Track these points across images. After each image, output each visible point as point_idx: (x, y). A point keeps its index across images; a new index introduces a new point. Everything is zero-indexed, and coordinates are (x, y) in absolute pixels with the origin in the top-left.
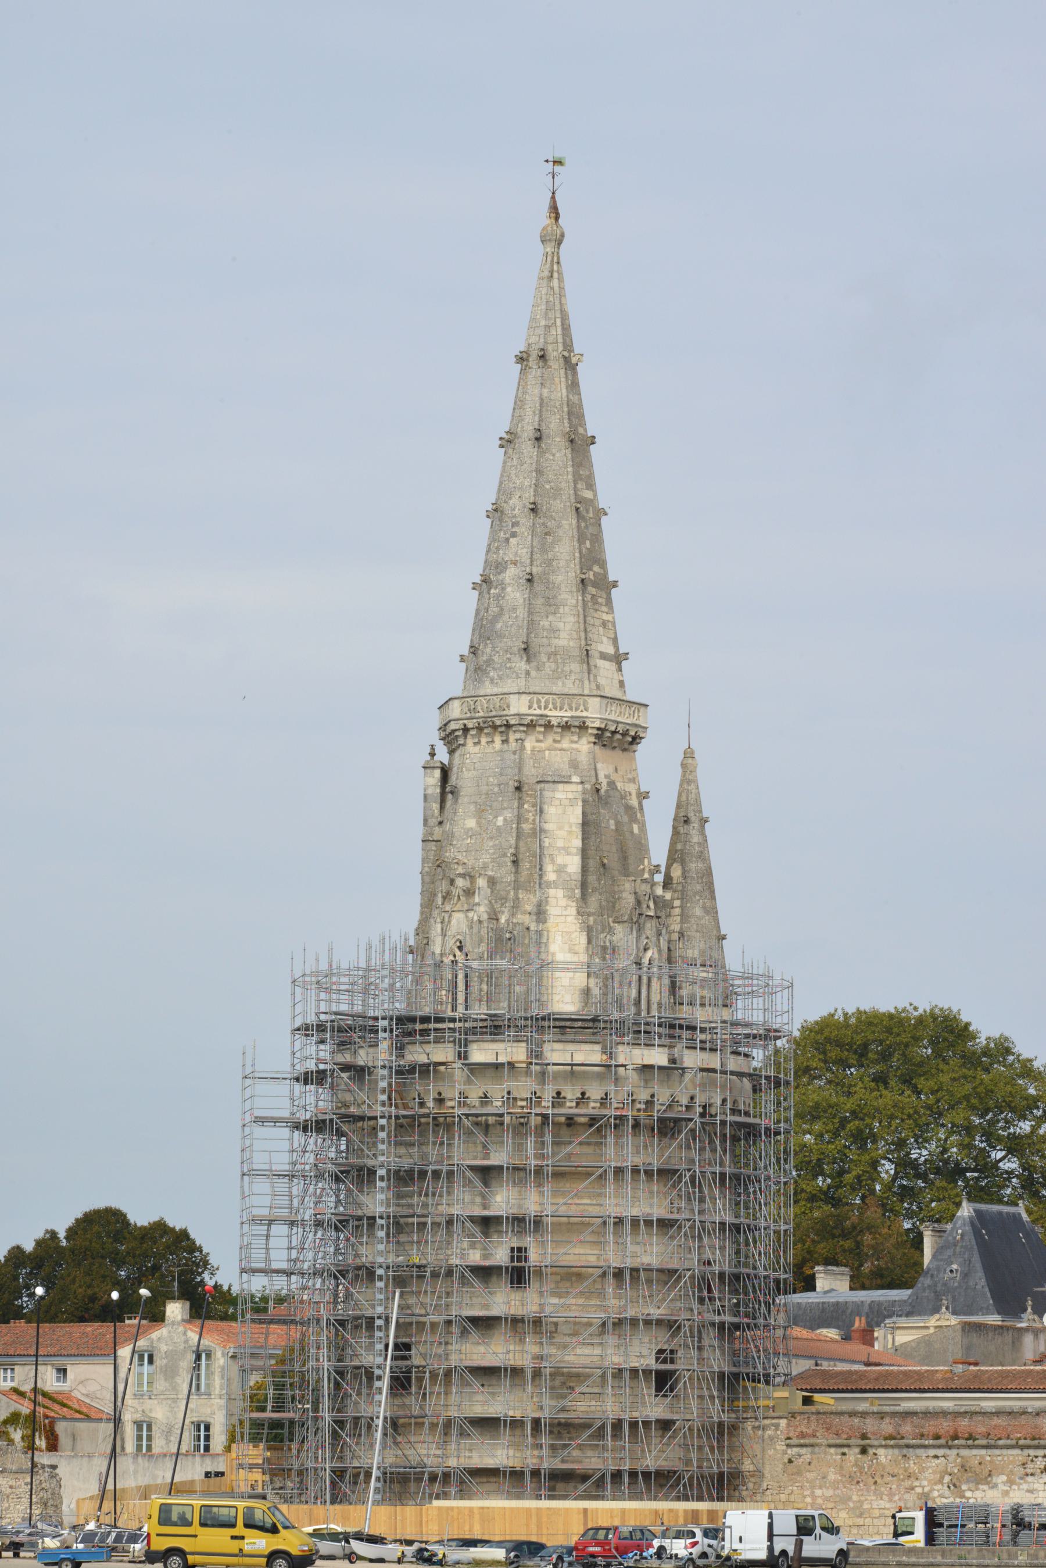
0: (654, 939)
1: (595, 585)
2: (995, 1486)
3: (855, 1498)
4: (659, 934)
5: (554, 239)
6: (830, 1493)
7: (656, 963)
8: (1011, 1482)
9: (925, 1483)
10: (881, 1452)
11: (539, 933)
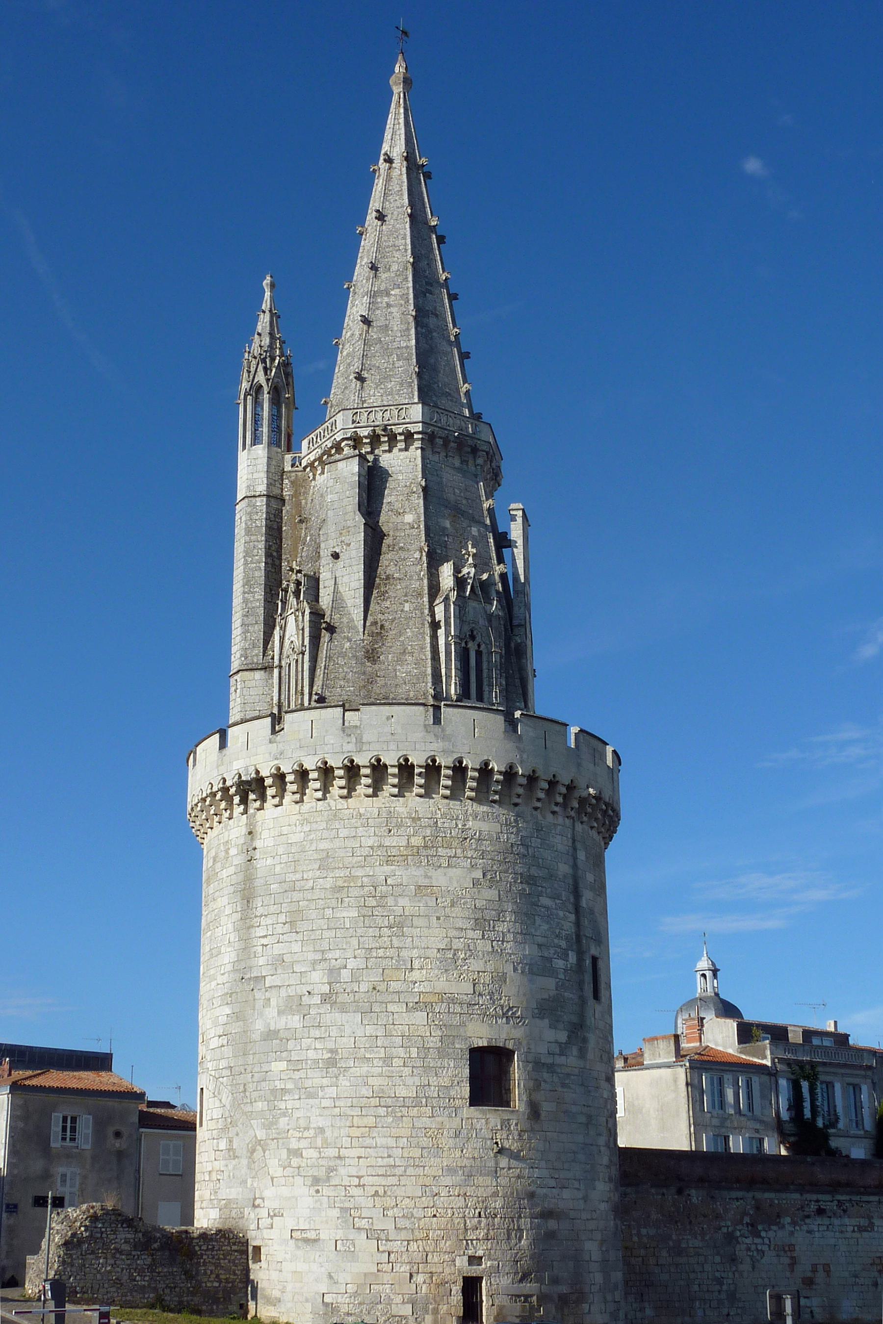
2: (783, 1227)
3: (674, 1237)
6: (652, 1232)
8: (794, 1223)
9: (729, 1223)
10: (693, 1192)
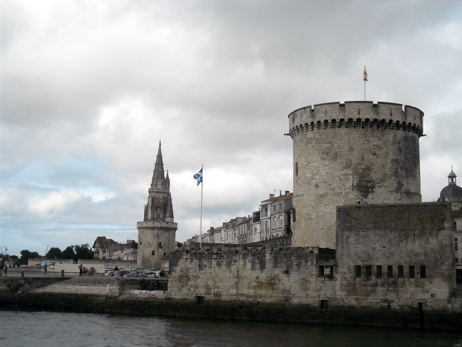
5: (160, 145)
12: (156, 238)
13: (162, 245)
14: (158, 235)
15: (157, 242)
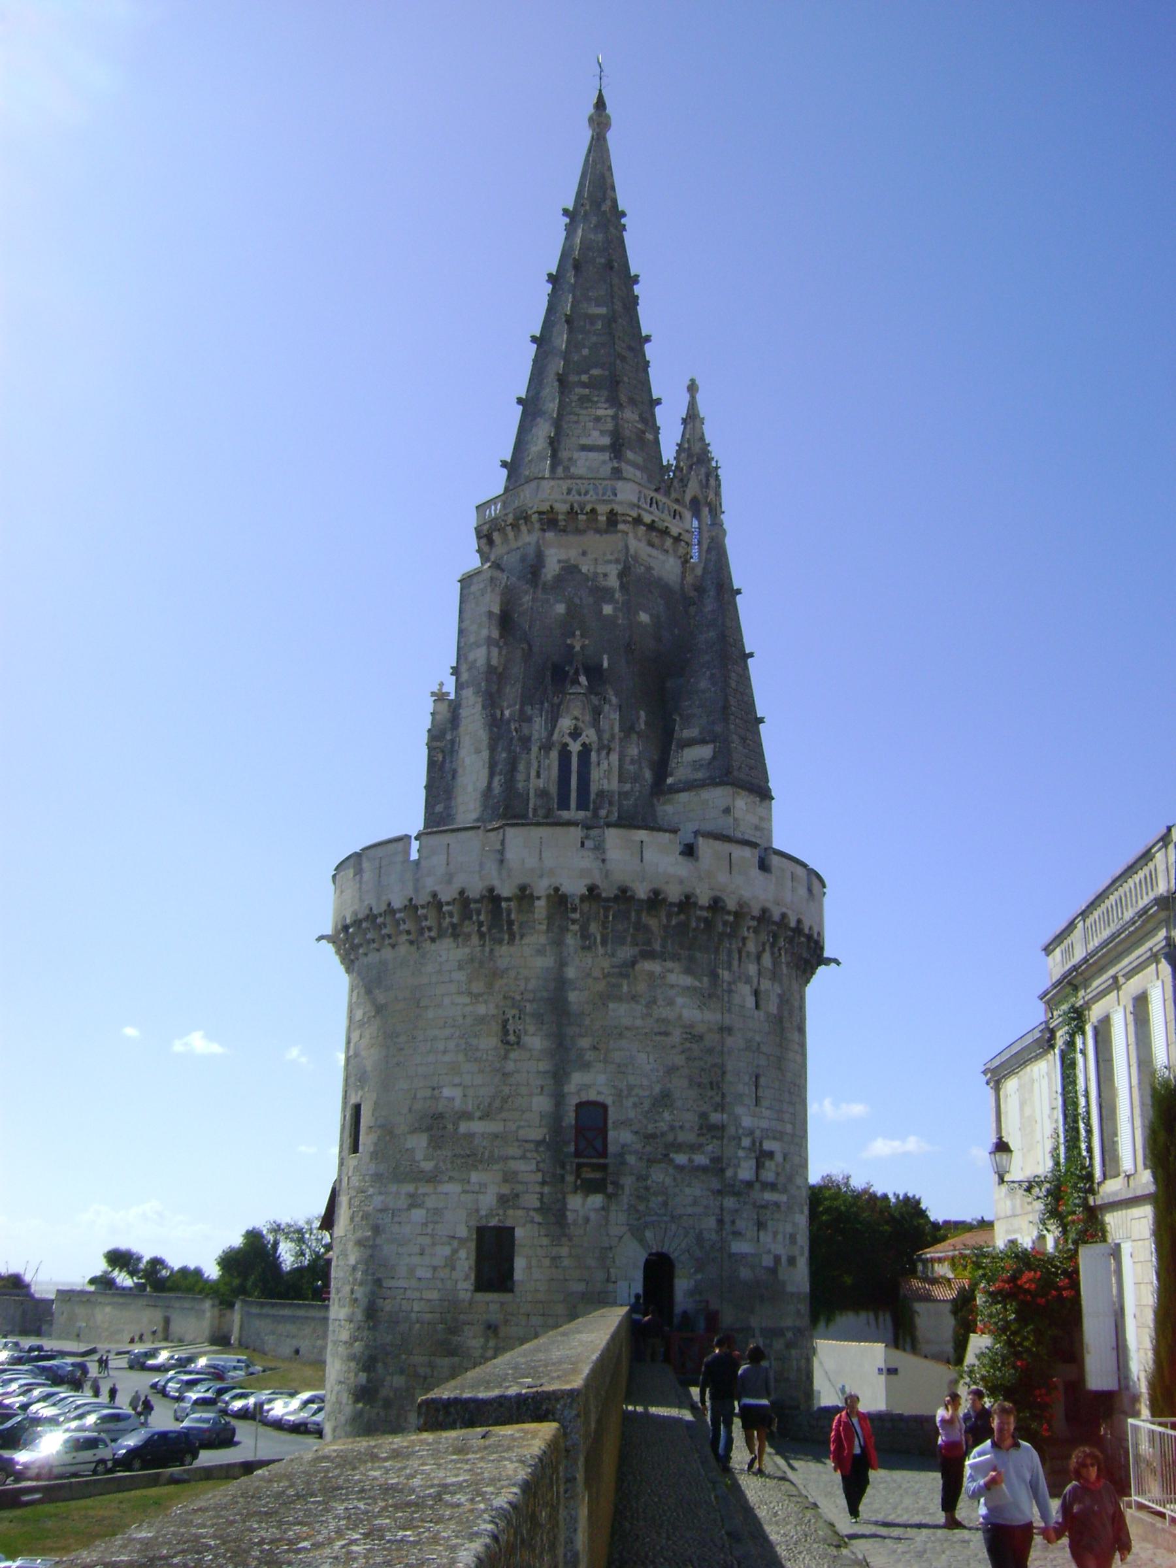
0: (587, 718)
1: (584, 385)
4: (597, 713)
7: (595, 747)
11: (453, 742)
12: (536, 1042)
13: (619, 1137)
14: (556, 1008)
15: (541, 1103)
